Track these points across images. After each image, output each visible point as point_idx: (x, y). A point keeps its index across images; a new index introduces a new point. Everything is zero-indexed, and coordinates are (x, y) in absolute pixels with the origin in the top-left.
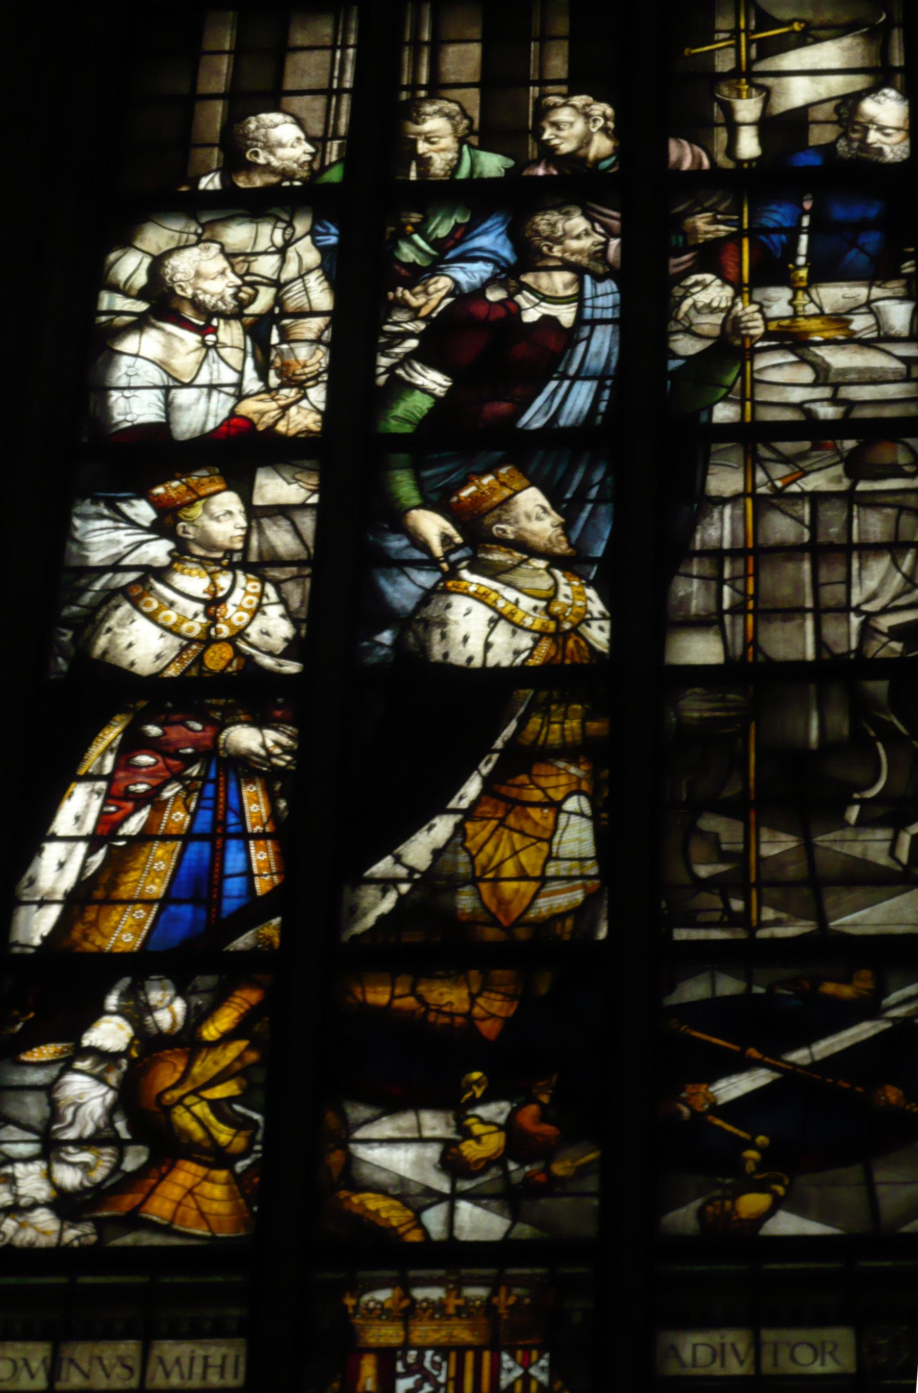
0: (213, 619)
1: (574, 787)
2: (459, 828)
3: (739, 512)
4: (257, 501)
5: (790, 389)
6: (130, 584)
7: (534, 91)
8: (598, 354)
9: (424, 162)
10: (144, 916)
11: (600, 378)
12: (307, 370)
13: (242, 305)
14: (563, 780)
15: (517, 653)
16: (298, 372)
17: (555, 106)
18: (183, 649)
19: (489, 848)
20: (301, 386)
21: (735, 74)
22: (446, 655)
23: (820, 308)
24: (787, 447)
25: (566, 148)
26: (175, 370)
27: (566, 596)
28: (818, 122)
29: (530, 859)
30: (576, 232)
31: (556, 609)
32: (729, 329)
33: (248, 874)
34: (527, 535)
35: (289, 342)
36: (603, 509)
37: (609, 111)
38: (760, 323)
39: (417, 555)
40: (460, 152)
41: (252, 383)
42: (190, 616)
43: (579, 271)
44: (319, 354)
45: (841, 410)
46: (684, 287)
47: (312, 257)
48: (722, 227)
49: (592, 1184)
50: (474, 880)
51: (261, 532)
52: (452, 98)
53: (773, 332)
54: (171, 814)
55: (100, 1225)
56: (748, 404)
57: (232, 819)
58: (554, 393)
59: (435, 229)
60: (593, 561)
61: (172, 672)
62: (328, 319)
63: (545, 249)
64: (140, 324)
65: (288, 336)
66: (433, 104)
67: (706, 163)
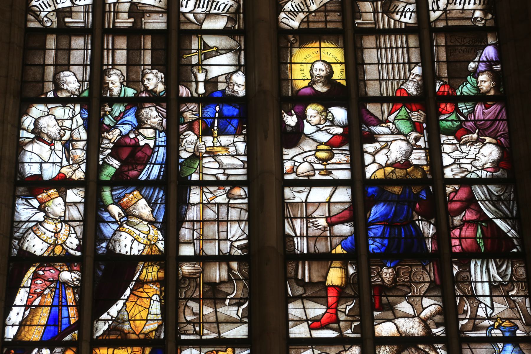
0: (57, 238)
1: (155, 293)
2: (124, 304)
3: (199, 208)
4: (67, 201)
6: (33, 226)
9: (111, 90)
10: (41, 329)
11: (161, 164)
12: (80, 159)
13: (61, 137)
14: (152, 290)
15: (139, 251)
17: (148, 73)
18: (49, 247)
19: (133, 310)
22: (120, 251)
24: (212, 189)
25: (151, 88)
27: (152, 233)
29: (144, 314)
30: (154, 117)
31: (150, 237)
32: (196, 150)
33: (69, 317)
34: (142, 214)
36: (162, 206)
37: (163, 76)
38: (204, 148)
40: (121, 87)
41: (65, 163)
43: (155, 129)
44: (83, 154)
45: (226, 177)
47: (81, 122)
48: (194, 116)
50: (129, 320)
51: (69, 210)
54: (47, 299)
56: (201, 174)
57: (64, 301)
58: (149, 168)
60: (159, 223)
61: (46, 254)
62: (86, 142)
64: (32, 141)
67: (190, 95)
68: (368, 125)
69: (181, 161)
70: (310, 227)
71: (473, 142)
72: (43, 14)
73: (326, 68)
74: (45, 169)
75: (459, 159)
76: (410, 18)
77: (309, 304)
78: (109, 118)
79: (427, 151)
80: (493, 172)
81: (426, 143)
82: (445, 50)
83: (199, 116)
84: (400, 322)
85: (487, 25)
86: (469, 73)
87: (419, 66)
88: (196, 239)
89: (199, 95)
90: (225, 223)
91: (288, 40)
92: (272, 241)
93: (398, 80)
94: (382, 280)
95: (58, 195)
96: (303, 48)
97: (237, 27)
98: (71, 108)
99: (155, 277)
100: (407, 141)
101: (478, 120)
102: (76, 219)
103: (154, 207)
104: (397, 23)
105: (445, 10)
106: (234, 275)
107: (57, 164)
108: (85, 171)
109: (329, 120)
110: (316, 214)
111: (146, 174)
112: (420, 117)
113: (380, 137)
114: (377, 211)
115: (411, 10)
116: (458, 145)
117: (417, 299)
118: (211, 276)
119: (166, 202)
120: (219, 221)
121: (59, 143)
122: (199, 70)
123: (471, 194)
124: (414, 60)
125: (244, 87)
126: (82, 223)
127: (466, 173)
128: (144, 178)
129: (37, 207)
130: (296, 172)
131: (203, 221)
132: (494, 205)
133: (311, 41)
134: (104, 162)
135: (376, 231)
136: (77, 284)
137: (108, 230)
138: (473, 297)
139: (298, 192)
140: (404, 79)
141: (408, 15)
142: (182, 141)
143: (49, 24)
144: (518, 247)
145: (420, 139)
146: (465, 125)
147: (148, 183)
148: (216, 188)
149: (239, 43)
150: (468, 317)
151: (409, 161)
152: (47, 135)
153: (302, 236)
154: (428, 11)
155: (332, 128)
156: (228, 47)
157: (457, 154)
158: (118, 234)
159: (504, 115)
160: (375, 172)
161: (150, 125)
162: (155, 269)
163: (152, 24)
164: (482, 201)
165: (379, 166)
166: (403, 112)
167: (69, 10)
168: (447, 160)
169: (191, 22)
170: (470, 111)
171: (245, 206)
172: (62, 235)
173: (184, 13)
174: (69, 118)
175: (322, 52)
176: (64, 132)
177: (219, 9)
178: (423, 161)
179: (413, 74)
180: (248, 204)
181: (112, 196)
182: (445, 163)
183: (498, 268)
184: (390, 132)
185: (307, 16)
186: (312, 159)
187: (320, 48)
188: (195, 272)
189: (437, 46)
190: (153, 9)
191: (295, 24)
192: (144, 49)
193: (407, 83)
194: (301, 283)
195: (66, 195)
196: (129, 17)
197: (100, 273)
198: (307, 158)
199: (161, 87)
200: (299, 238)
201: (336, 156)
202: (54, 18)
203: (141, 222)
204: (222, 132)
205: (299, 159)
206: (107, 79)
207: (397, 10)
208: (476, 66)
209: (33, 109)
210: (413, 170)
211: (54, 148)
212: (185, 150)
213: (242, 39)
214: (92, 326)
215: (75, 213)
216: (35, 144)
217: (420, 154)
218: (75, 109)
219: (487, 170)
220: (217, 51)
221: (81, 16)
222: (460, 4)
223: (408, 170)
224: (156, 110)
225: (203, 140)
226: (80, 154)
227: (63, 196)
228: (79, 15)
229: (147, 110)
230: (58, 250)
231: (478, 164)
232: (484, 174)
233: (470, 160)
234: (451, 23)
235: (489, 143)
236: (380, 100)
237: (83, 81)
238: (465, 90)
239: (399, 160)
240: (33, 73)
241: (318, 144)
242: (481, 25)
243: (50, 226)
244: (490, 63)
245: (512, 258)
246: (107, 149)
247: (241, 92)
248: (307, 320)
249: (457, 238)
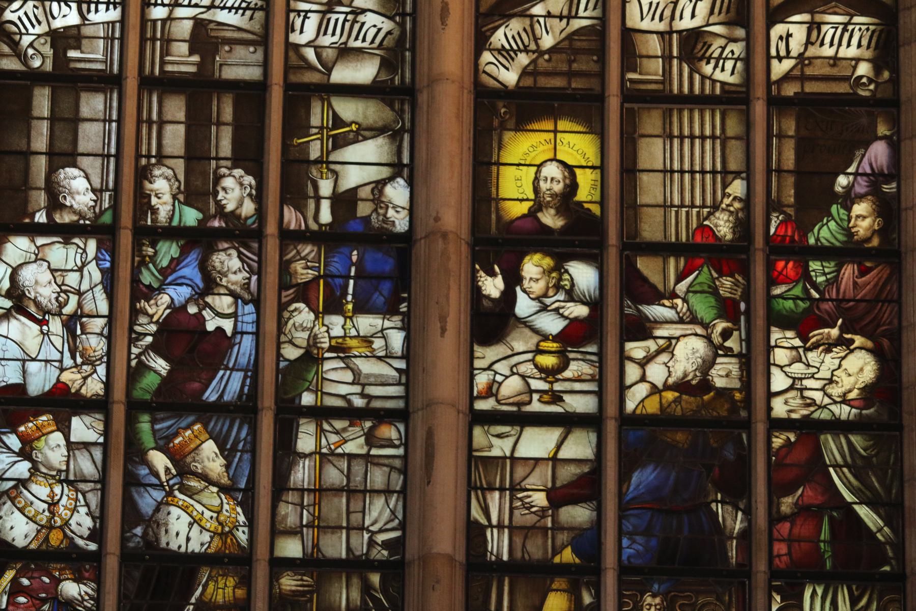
0: (53, 513)
3: (313, 464)
4: (73, 439)
5: (341, 385)
6: (10, 489)
7: (213, 163)
8: (244, 354)
9: (155, 211)
11: (246, 370)
12: (96, 354)
13: (61, 306)
15: (202, 545)
16: (91, 355)
17: (224, 176)
18: (38, 531)
20: (92, 364)
21: (319, 161)
22: (168, 544)
23: (358, 332)
24: (339, 424)
25: (230, 207)
26: (27, 349)
27: (227, 511)
28: (362, 200)
30: (234, 270)
31: (222, 518)
32: (311, 342)
34: (207, 470)
35: (86, 334)
37: (253, 182)
38: (327, 340)
39: (154, 481)
41: (68, 362)
42: (41, 512)
44: (102, 343)
45: (365, 401)
46: (289, 312)
47: (97, 276)
48: (310, 271)
52: (169, 165)
53: (333, 346)
56: (319, 393)
58: (222, 378)
59: (161, 261)
60: (240, 490)
63: (218, 279)
65: (85, 330)
66: (159, 169)
70: (517, 508)
71: (829, 344)
72: (26, 40)
73: (565, 177)
74: (31, 374)
75: (801, 379)
76: (732, 73)
78: (149, 269)
79: (744, 360)
80: (861, 409)
81: (744, 343)
82: (793, 146)
83: (319, 272)
85: (879, 96)
87: (742, 179)
88: (306, 526)
89: (321, 225)
90: (360, 496)
93: (699, 207)
95: (54, 428)
96: (522, 131)
98: (79, 247)
100: (708, 338)
101: (844, 300)
102: (89, 478)
103: (230, 458)
104: (708, 82)
105: (801, 56)
107: (53, 363)
108: (104, 379)
109: (563, 287)
110: (527, 483)
111: (217, 389)
112: (735, 288)
113: (658, 328)
114: (643, 478)
115: (735, 56)
116: (801, 350)
118: (332, 599)
120: (350, 492)
121: (58, 319)
122: (322, 173)
123: (817, 453)
124: (733, 166)
125: (406, 212)
126: (99, 486)
127: (812, 409)
128: (213, 398)
129: (17, 450)
130: (496, 395)
131: (320, 491)
133: (538, 116)
134: (141, 364)
136: (89, 605)
137: (147, 501)
139: (499, 436)
140: (710, 207)
141: (729, 65)
142: (286, 323)
143: (37, 63)
144: (893, 562)
145: (731, 334)
146: (818, 308)
147: (220, 408)
148: (346, 423)
151: (709, 379)
153: (500, 526)
154: (769, 58)
155: (569, 304)
157: (798, 369)
158: (164, 509)
160: (643, 401)
161: (226, 287)
163: (234, 68)
164: (836, 466)
165: (651, 388)
166: (705, 275)
167: (75, 31)
168: (779, 382)
169: (310, 67)
170: (831, 278)
171: (397, 463)
172: (62, 508)
174: (76, 268)
175: (558, 141)
176: (65, 297)
177: (364, 40)
178: (733, 381)
179: (730, 195)
181: (154, 432)
184: (678, 319)
185: (534, 62)
186: (527, 368)
187: (555, 131)
188: (304, 591)
190: (237, 35)
191: (510, 77)
192: (219, 124)
193: (717, 214)
195: (69, 427)
196: (192, 52)
198: (518, 367)
199: (248, 208)
200: (495, 531)
201: (573, 366)
202: (48, 50)
203: (207, 487)
204: (362, 308)
205: (500, 367)
206: (148, 185)
207: (708, 54)
208: (849, 182)
209: (9, 246)
210: (714, 398)
211: (48, 331)
212: (291, 342)
215: (86, 465)
216: (13, 322)
217: (730, 367)
218: (88, 250)
219: (852, 403)
220: (357, 132)
221: (98, 46)
222: (831, 44)
223: (706, 397)
224: (239, 257)
225: (326, 322)
226: (96, 344)
227: (65, 429)
228: (95, 44)
229: (222, 256)
230: (55, 538)
232: (844, 412)
233: (822, 383)
234: (811, 87)
235: (861, 348)
237: (101, 191)
238: (825, 233)
239: (690, 378)
241: (540, 338)
242: (867, 94)
243: (41, 490)
244: (876, 178)
246: (146, 335)
247: (401, 222)
249: (783, 540)
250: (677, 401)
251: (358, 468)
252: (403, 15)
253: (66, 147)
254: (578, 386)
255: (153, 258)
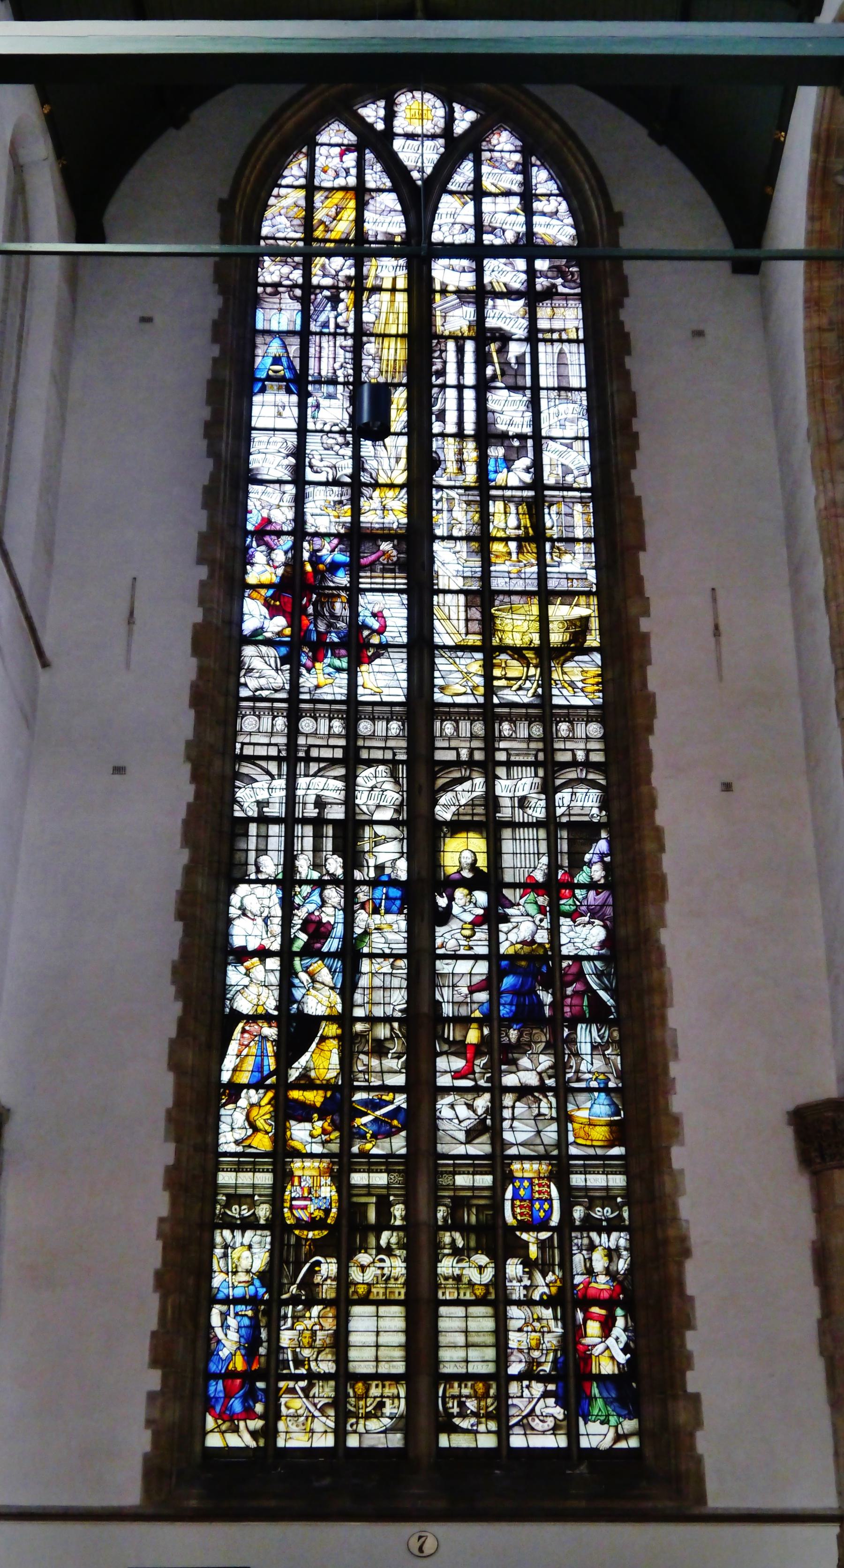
9: (300, 873)
10: (248, 1074)
24: (379, 960)
29: (326, 1064)
39: (301, 985)
41: (265, 936)
43: (335, 908)
47: (277, 900)
49: (338, 1141)
55: (244, 1147)
64: (239, 917)
68: (504, 907)
69: (355, 936)
77: (453, 1059)
84: (520, 1074)
86: (585, 863)
91: (442, 831)
92: (425, 1009)
94: (509, 1040)
97: (401, 818)
99: (334, 1034)
100: (534, 922)
105: (569, 807)
106: (395, 1033)
117: (535, 1056)
119: (344, 971)
132: (598, 978)
134: (295, 936)
135: (506, 998)
137: (298, 993)
138: (577, 1055)
143: (250, 814)
147: (329, 955)
148: (382, 960)
149: (402, 832)
150: (573, 1070)
152: (252, 913)
153: (448, 1002)
154: (555, 807)
156: (394, 836)
157: (572, 934)
159: (610, 901)
162: (335, 1026)
166: (531, 896)
168: (564, 939)
169: (365, 813)
173: (358, 805)
180: (408, 974)
182: (562, 942)
183: (599, 1030)
186: (459, 936)
189: (561, 838)
192: (327, 837)
194: (447, 1041)
196: (315, 808)
197: (292, 1030)
199: (339, 872)
202: (256, 809)
204: (388, 911)
205: (448, 936)
213: (405, 829)
214: (287, 1073)
215: (274, 979)
226: (277, 929)
230: (260, 1010)
231: (587, 943)
232: (592, 952)
234: (573, 819)
236: (514, 886)
240: (239, 856)
243: (253, 989)
244: (602, 856)
245: (610, 1024)
247: (403, 876)
248: (450, 1072)
250: (522, 948)
251: (388, 978)
252: (403, 791)
253: (262, 847)
254: (480, 943)
255: (300, 893)
